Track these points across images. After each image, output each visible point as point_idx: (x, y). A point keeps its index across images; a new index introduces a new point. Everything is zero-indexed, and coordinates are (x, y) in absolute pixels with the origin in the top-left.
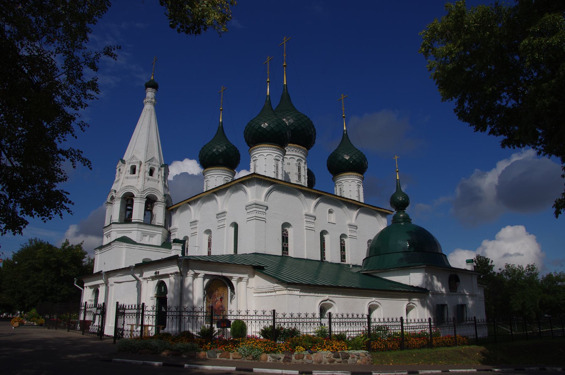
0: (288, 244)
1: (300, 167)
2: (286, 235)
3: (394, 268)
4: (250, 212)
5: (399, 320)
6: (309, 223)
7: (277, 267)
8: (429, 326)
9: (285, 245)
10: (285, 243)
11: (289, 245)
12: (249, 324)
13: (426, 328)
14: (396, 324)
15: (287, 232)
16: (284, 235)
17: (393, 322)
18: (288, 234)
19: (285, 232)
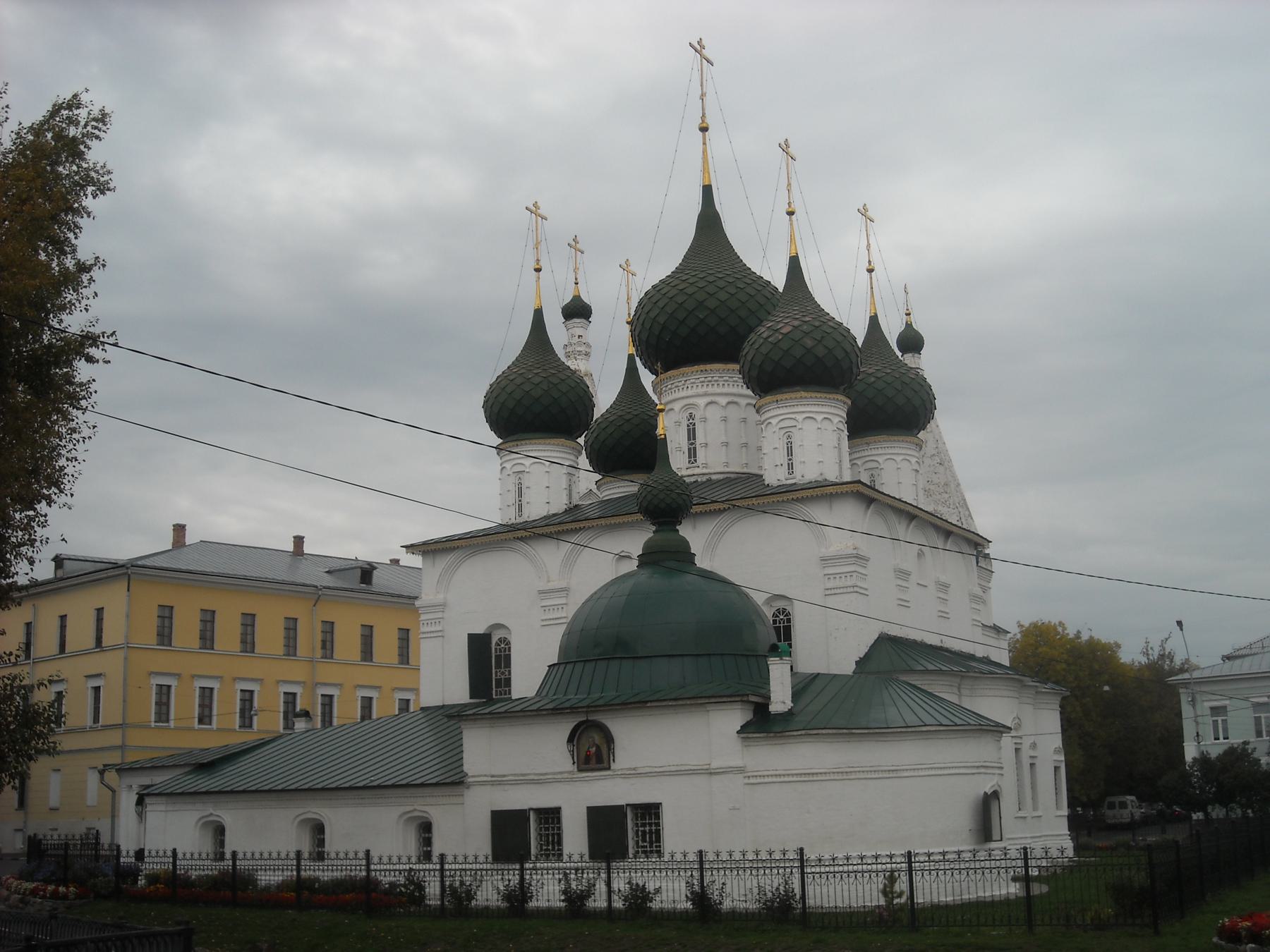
0: (510, 672)
1: (694, 425)
2: (505, 651)
3: (675, 699)
4: (428, 620)
5: (169, 853)
6: (551, 608)
7: (432, 739)
8: (294, 867)
9: (503, 673)
10: (503, 670)
11: (512, 674)
12: (918, 878)
13: (208, 869)
14: (163, 860)
15: (507, 644)
16: (500, 651)
17: (253, 859)
18: (510, 650)
19: (503, 646)
